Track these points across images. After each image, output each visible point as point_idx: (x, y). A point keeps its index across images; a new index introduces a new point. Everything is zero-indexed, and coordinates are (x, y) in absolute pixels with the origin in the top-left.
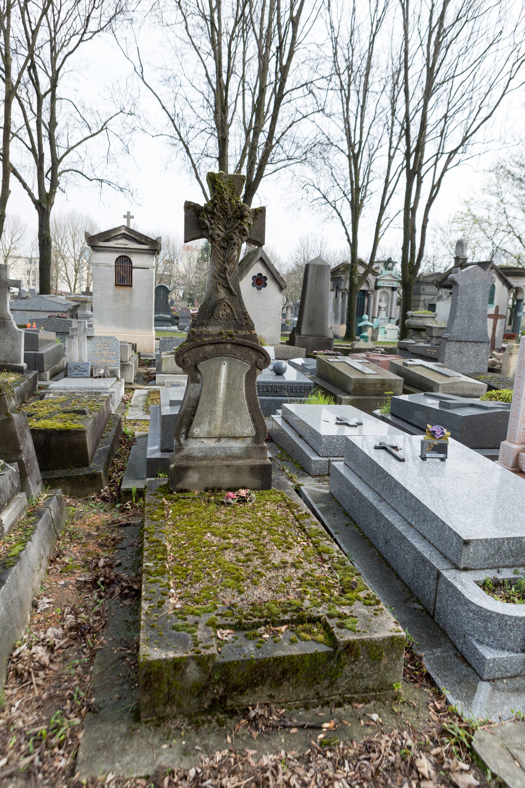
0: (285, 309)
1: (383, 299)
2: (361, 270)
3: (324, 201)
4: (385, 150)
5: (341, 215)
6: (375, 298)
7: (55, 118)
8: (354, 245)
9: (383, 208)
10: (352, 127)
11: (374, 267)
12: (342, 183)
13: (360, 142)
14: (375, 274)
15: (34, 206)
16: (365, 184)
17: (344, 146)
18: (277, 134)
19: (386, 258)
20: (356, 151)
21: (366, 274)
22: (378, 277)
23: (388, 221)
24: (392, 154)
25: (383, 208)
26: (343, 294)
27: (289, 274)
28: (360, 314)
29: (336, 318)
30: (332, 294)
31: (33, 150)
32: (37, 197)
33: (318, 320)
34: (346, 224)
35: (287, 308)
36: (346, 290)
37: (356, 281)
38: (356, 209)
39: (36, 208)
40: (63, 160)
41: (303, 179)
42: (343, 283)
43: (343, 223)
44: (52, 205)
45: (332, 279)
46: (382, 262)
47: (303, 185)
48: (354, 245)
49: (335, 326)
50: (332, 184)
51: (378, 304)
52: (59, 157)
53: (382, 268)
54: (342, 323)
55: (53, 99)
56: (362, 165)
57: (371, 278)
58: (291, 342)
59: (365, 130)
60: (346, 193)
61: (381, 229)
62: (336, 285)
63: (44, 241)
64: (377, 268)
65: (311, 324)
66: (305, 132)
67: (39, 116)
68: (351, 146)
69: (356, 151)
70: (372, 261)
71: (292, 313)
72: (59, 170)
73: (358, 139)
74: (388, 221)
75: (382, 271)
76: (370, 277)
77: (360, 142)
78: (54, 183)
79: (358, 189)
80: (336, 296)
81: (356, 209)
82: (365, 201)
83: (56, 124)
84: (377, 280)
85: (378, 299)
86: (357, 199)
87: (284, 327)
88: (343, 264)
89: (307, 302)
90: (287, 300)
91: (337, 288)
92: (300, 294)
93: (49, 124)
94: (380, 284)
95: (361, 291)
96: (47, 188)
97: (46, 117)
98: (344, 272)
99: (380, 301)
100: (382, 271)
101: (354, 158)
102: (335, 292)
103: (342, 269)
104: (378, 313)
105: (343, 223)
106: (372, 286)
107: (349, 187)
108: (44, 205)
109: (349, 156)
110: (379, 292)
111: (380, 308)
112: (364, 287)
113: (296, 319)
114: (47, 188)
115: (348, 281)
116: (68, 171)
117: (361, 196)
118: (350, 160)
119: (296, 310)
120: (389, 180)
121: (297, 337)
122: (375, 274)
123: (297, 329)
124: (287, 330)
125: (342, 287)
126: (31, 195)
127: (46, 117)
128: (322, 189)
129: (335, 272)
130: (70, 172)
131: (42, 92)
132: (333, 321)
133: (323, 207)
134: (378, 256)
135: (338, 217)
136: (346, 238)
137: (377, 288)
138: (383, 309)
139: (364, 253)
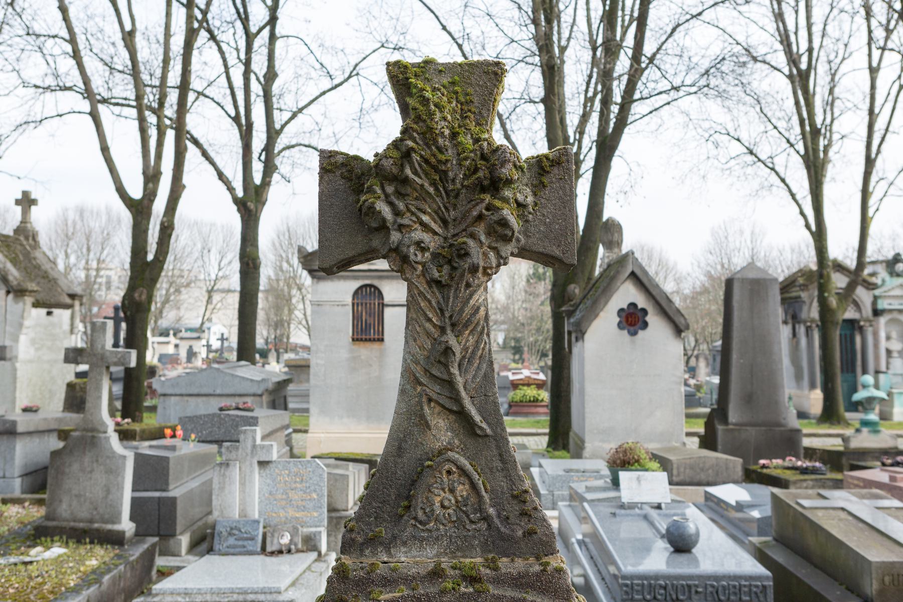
0: (693, 360)
1: (894, 335)
2: (839, 281)
3: (750, 159)
4: (859, 60)
5: (788, 181)
6: (876, 334)
7: (273, 67)
8: (819, 236)
9: (870, 163)
10: (791, 27)
11: (867, 271)
12: (782, 125)
13: (810, 50)
14: (870, 286)
15: (235, 208)
16: (828, 121)
17: (780, 59)
18: (649, 48)
19: (890, 255)
20: (804, 66)
21: (851, 288)
22: (877, 292)
23: (883, 185)
24: (875, 64)
25: (870, 163)
26: (808, 330)
27: (695, 296)
28: (849, 366)
29: (798, 377)
30: (785, 332)
31: (236, 119)
32: (240, 193)
33: (762, 392)
34: (798, 197)
35: (697, 357)
36: (813, 321)
37: (833, 302)
38: (815, 167)
39: (239, 210)
40: (286, 129)
41: (706, 125)
42: (805, 308)
43: (793, 196)
44: (264, 204)
45: (784, 301)
46: (882, 262)
47: (707, 135)
48: (819, 236)
49: (798, 392)
50: (762, 128)
51: (883, 344)
52: (278, 126)
53: (883, 274)
54: (813, 386)
55: (273, 38)
56: (818, 89)
57: (861, 293)
58: (708, 441)
59: (817, 29)
60: (792, 140)
61: (872, 202)
62: (791, 311)
63: (248, 264)
64: (873, 274)
65: (749, 399)
66: (703, 42)
67: (247, 63)
68: (793, 60)
69: (804, 66)
70: (861, 263)
71: (708, 365)
72: (278, 147)
73: (804, 46)
74: (883, 185)
75: (884, 281)
76: (861, 293)
77: (810, 50)
78: (269, 168)
79: (816, 132)
80: (794, 334)
81: (815, 167)
82: (831, 154)
83: (275, 75)
84: (876, 298)
85: (882, 335)
86: (816, 151)
87: (691, 400)
88: (800, 271)
89: (735, 356)
90: (696, 341)
91: (794, 318)
92: (720, 329)
93: (265, 76)
94: (882, 304)
95: (845, 321)
96: (257, 179)
97: (259, 65)
98: (804, 287)
99: (888, 338)
100: (884, 281)
101: (801, 79)
102: (790, 327)
103: (801, 281)
104: (888, 363)
105: (793, 196)
106: (868, 311)
107: (798, 130)
108: (251, 205)
109: (790, 77)
110: (882, 320)
111: (889, 352)
112: (850, 314)
113: (716, 380)
114: (257, 179)
115: (815, 304)
116: (293, 146)
117: (822, 143)
118: (793, 82)
119: (714, 360)
120: (877, 111)
121: (720, 428)
122: (870, 286)
123: (719, 413)
124: (700, 405)
125: (804, 315)
126: (231, 189)
127: (259, 65)
128: (744, 137)
129: (787, 286)
130: (297, 148)
131: (253, 29)
132: (793, 383)
133: (749, 170)
134: (872, 252)
135: (782, 185)
136: (802, 222)
137: (877, 313)
138: (895, 354)
139: (842, 246)
